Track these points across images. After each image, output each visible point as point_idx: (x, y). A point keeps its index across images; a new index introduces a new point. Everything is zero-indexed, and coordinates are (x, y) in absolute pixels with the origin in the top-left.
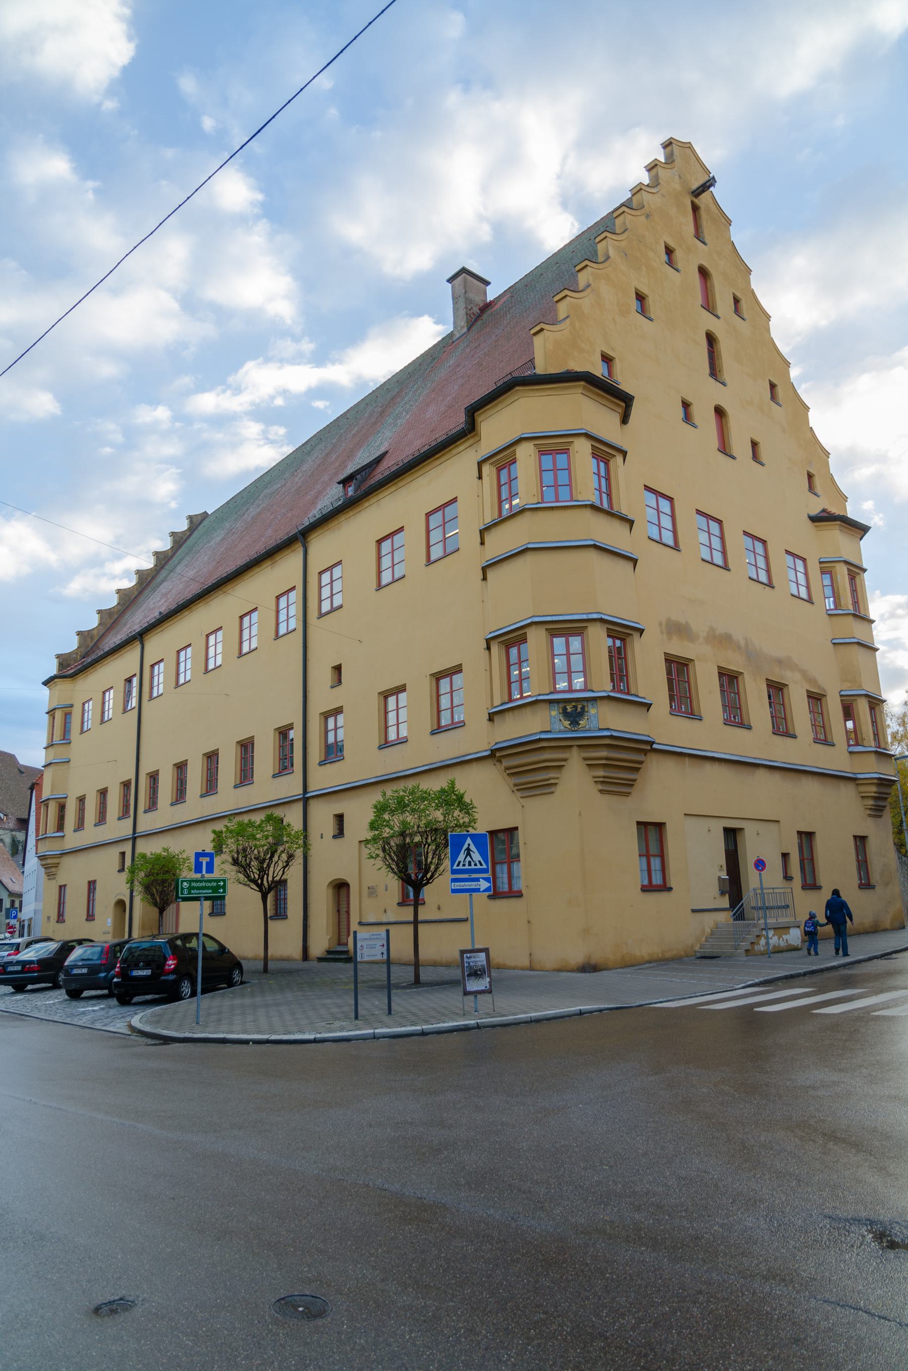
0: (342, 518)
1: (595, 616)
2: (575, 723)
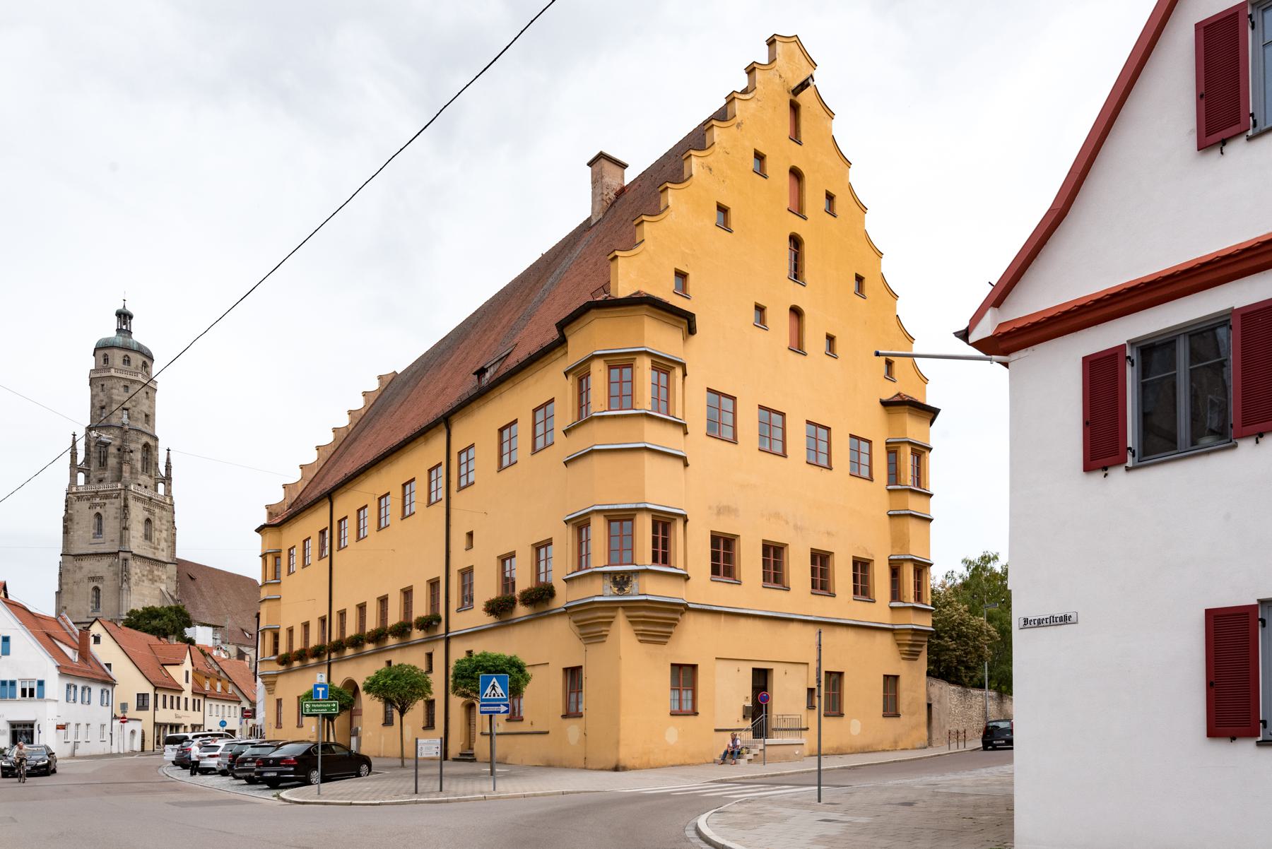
0: (474, 405)
1: (642, 506)
2: (621, 589)
